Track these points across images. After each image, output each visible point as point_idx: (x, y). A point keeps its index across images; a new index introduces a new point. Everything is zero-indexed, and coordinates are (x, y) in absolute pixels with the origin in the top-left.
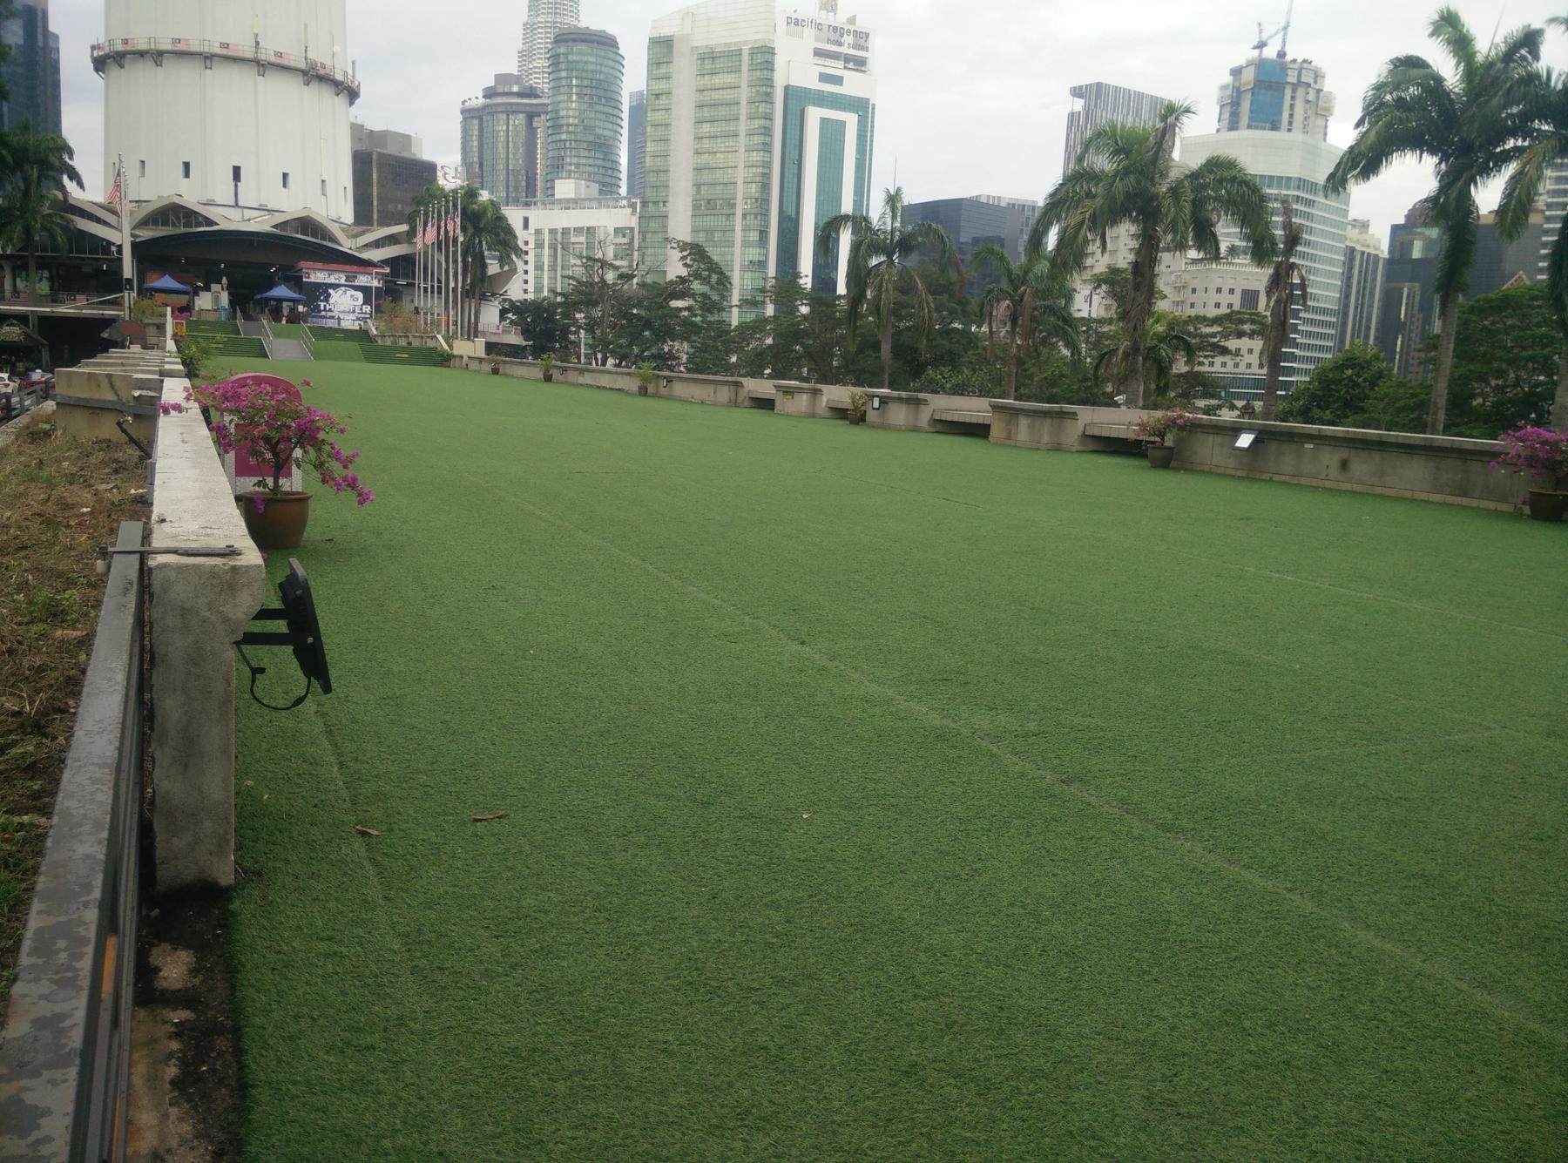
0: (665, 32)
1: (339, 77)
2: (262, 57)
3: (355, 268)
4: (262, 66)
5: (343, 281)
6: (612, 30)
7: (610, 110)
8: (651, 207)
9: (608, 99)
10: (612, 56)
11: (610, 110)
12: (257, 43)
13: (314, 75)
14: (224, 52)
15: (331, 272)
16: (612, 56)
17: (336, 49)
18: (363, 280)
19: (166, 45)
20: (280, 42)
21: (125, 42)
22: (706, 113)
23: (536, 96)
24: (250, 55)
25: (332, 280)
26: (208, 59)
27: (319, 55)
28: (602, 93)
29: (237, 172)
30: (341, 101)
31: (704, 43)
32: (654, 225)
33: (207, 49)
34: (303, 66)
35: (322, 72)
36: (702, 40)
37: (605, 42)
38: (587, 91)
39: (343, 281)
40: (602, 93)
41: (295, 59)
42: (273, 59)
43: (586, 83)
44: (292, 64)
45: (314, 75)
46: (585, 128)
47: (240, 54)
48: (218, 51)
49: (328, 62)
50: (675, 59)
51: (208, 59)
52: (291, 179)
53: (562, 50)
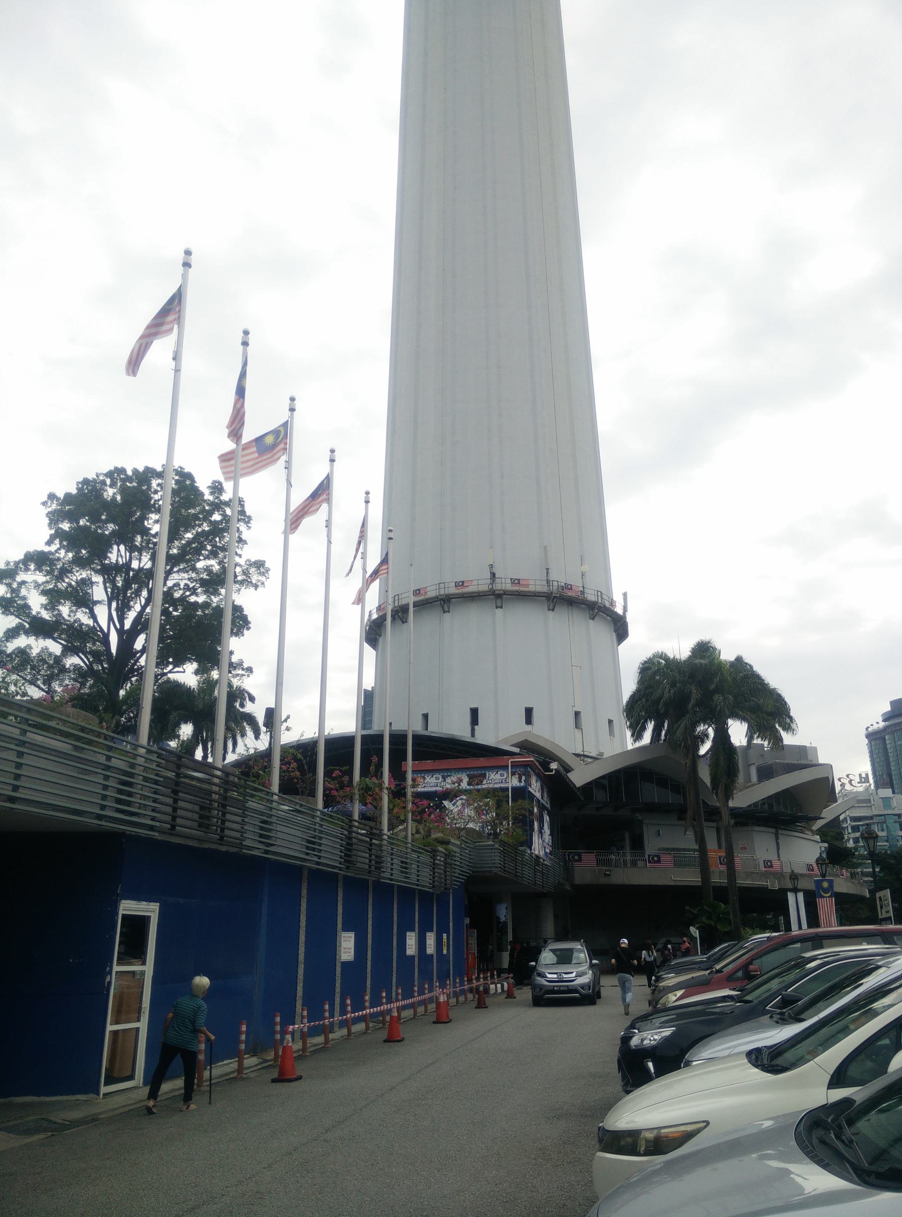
1: (591, 597)
3: (482, 762)
5: (464, 785)
12: (493, 575)
15: (446, 772)
17: (585, 568)
18: (495, 779)
20: (520, 567)
24: (484, 588)
25: (448, 785)
27: (564, 574)
29: (474, 712)
30: (601, 631)
33: (442, 592)
39: (464, 785)
41: (537, 585)
42: (509, 587)
44: (532, 588)
49: (577, 583)
51: (443, 603)
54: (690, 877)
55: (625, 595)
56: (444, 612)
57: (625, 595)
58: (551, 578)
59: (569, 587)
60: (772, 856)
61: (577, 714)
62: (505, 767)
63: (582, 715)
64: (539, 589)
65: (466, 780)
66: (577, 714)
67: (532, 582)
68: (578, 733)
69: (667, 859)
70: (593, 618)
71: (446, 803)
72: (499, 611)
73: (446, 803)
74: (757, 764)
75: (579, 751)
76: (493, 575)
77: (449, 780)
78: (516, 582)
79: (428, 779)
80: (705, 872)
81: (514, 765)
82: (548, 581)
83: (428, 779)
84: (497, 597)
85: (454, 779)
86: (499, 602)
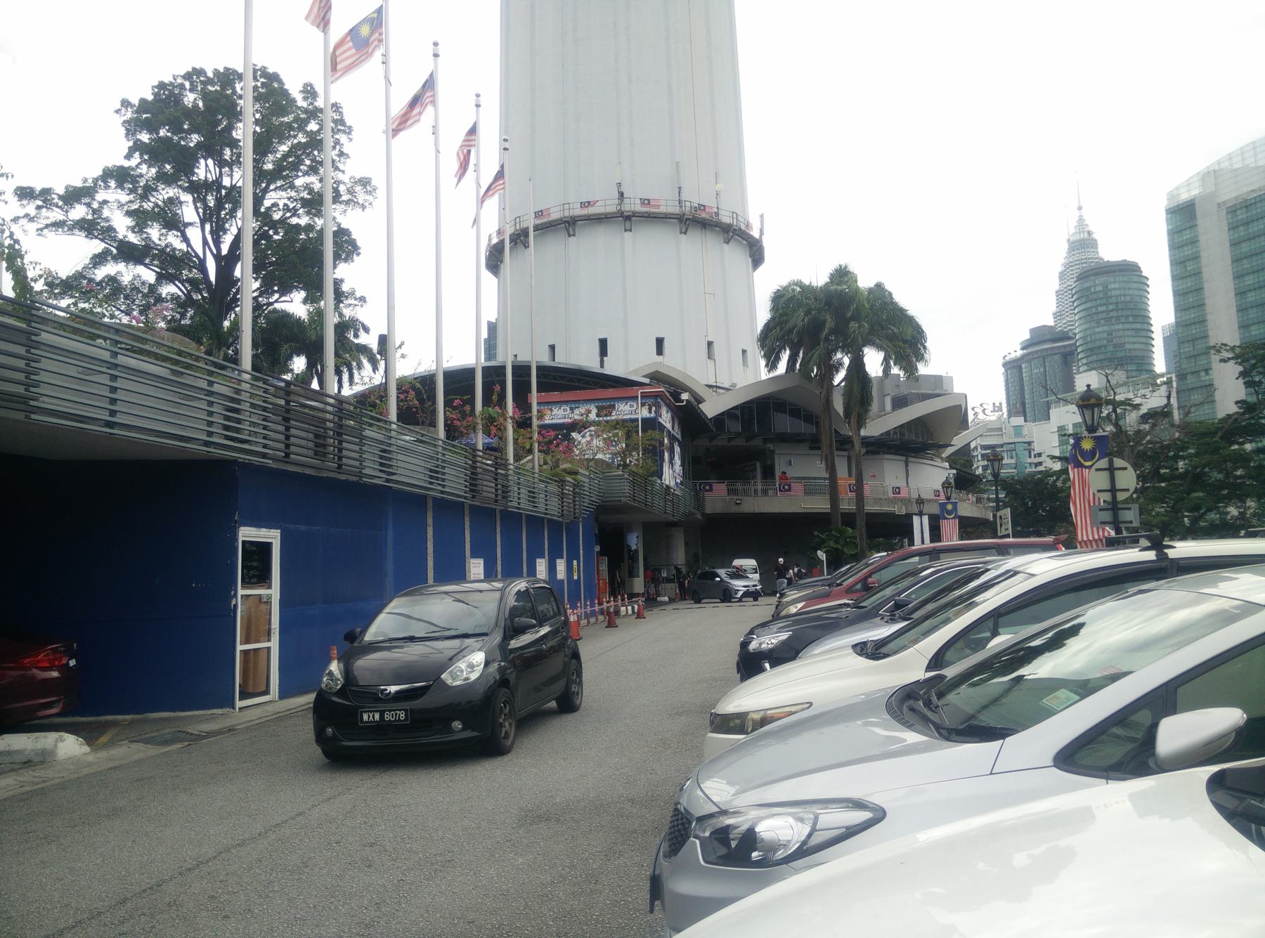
0: (1184, 196)
1: (725, 219)
3: (610, 393)
5: (593, 416)
6: (1130, 258)
7: (1139, 326)
8: (1191, 380)
9: (1135, 316)
10: (1136, 279)
11: (1139, 326)
12: (622, 194)
13: (696, 221)
14: (585, 212)
16: (1136, 279)
17: (719, 187)
18: (624, 410)
22: (1246, 264)
24: (612, 208)
25: (577, 415)
27: (697, 195)
28: (1129, 313)
29: (603, 344)
30: (735, 256)
31: (1234, 195)
32: (1196, 397)
33: (567, 214)
34: (677, 210)
36: (1229, 193)
37: (1129, 271)
38: (1112, 314)
39: (593, 416)
40: (1129, 313)
41: (668, 205)
42: (639, 208)
43: (1111, 307)
44: (663, 209)
45: (696, 221)
46: (1115, 346)
49: (710, 202)
50: (1200, 222)
51: (569, 225)
52: (666, 343)
53: (1086, 285)
54: (820, 504)
57: (762, 216)
58: (683, 199)
59: (702, 207)
60: (901, 483)
61: (710, 344)
62: (635, 398)
63: (716, 346)
64: (670, 210)
65: (594, 411)
66: (710, 344)
67: (663, 203)
68: (711, 363)
69: (797, 488)
71: (574, 435)
73: (574, 435)
74: (892, 394)
75: (712, 382)
76: (622, 194)
77: (577, 411)
79: (555, 411)
80: (834, 500)
81: (644, 396)
82: (680, 202)
83: (555, 411)
85: (582, 410)
86: (628, 224)
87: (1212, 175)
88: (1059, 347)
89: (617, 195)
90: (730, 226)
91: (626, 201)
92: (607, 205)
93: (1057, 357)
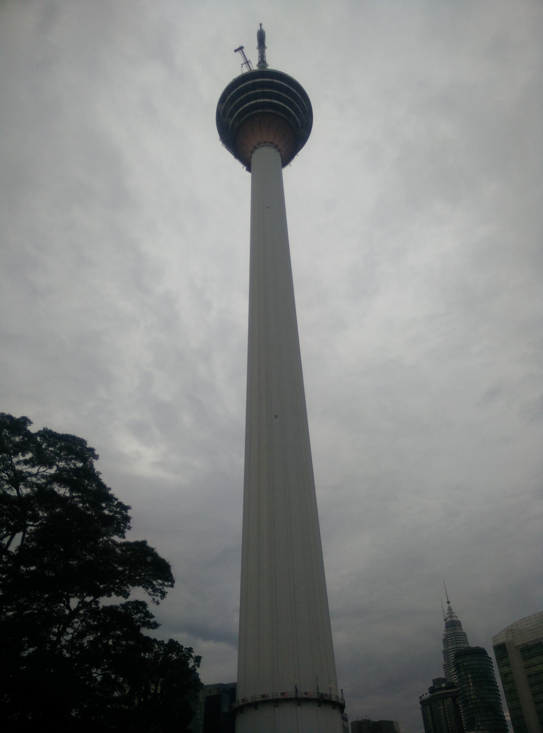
0: (500, 641)
1: (334, 699)
2: (299, 696)
4: (299, 701)
12: (296, 690)
17: (331, 685)
19: (259, 699)
20: (307, 688)
21: (243, 700)
23: (455, 687)
24: (293, 696)
26: (276, 702)
33: (275, 697)
34: (316, 697)
35: (326, 698)
37: (480, 652)
42: (304, 696)
44: (312, 697)
47: (289, 697)
48: (280, 697)
49: (328, 693)
51: (276, 702)
53: (459, 661)
55: (342, 690)
56: (275, 706)
57: (342, 690)
67: (312, 694)
70: (334, 708)
72: (299, 708)
76: (296, 690)
78: (306, 693)
82: (318, 693)
84: (299, 701)
87: (509, 630)
88: (449, 693)
89: (295, 691)
90: (335, 702)
91: (299, 693)
92: (290, 692)
93: (450, 699)
